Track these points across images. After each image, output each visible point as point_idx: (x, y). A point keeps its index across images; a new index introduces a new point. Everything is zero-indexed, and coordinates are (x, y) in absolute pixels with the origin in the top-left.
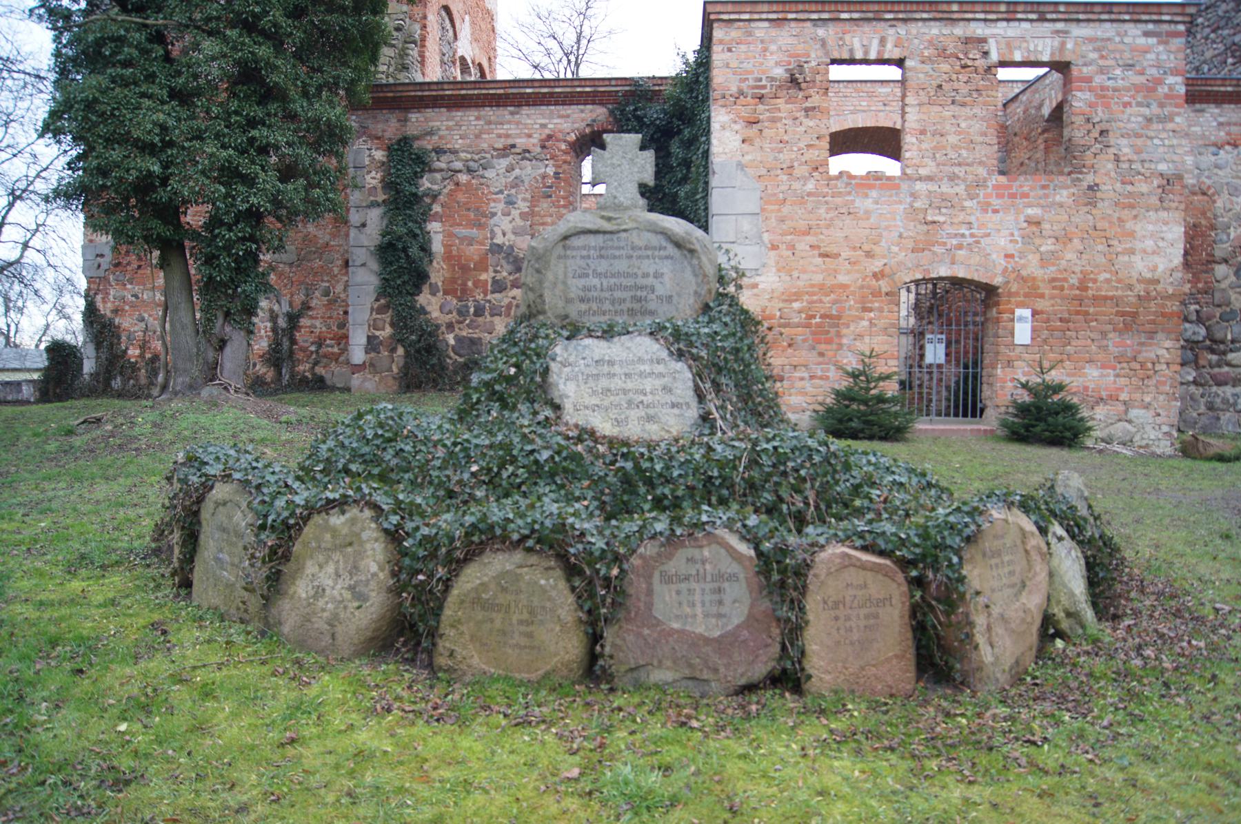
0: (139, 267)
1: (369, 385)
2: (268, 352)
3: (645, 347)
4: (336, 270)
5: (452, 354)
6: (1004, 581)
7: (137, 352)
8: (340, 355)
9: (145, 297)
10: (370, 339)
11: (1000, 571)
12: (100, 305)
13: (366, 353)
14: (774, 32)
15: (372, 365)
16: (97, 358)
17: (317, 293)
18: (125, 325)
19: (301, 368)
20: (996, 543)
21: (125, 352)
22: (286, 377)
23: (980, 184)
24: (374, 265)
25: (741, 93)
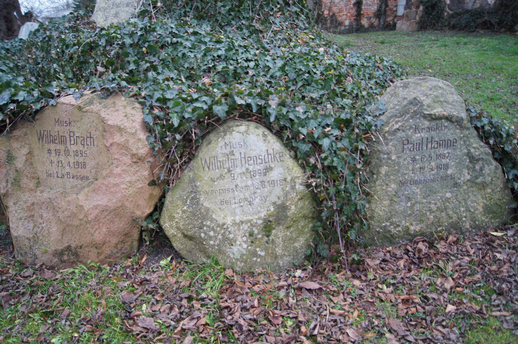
1: (404, 27)
5: (447, 9)
6: (67, 169)
11: (62, 158)
13: (405, 9)
15: (407, 16)
20: (57, 128)
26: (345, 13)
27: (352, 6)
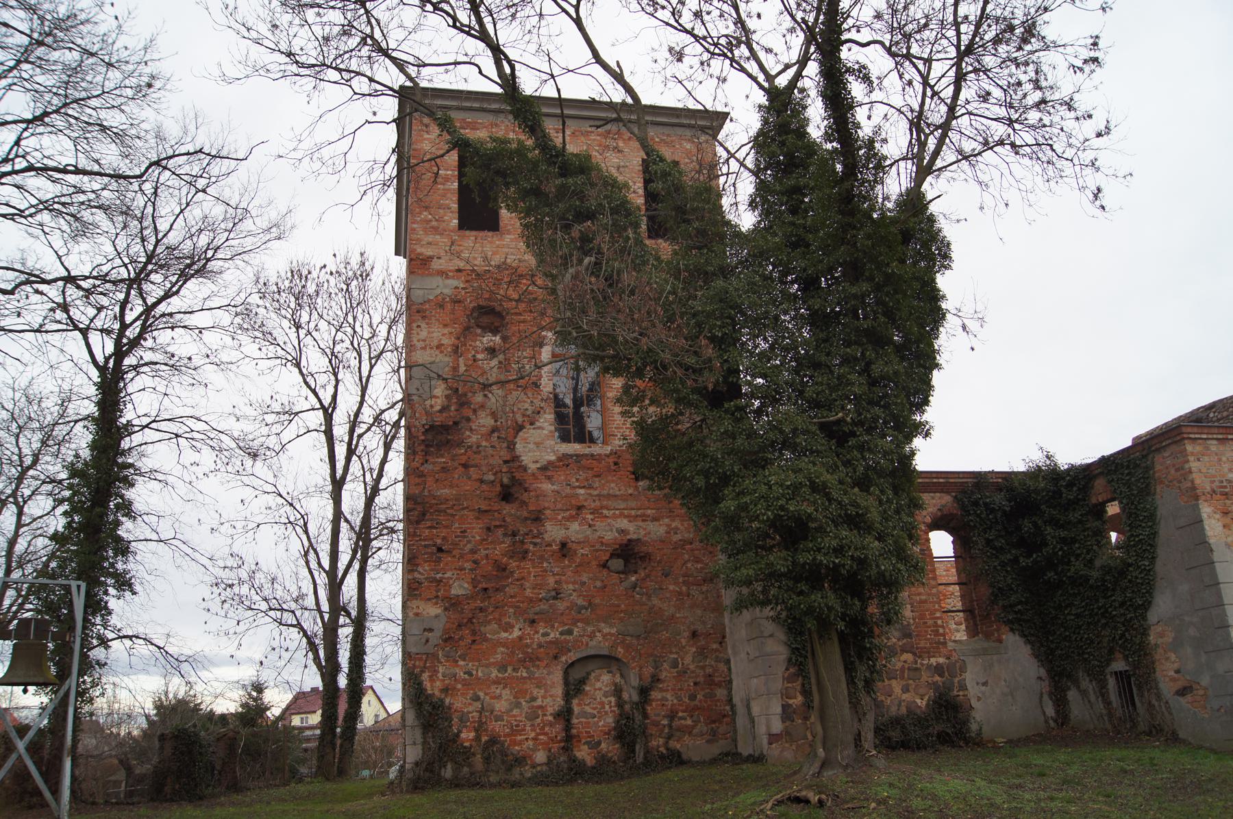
0: (474, 641)
1: (788, 755)
2: (615, 729)
4: (684, 642)
7: (472, 735)
8: (693, 727)
9: (480, 674)
10: (785, 707)
12: (427, 685)
13: (783, 722)
14: (1221, 448)
16: (424, 743)
17: (665, 665)
18: (458, 705)
19: (654, 743)
21: (458, 735)
22: (640, 757)
24: (781, 635)
26: (533, 735)
27: (551, 718)
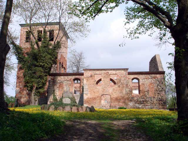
3: (68, 99)
23: (108, 85)
25: (86, 77)
